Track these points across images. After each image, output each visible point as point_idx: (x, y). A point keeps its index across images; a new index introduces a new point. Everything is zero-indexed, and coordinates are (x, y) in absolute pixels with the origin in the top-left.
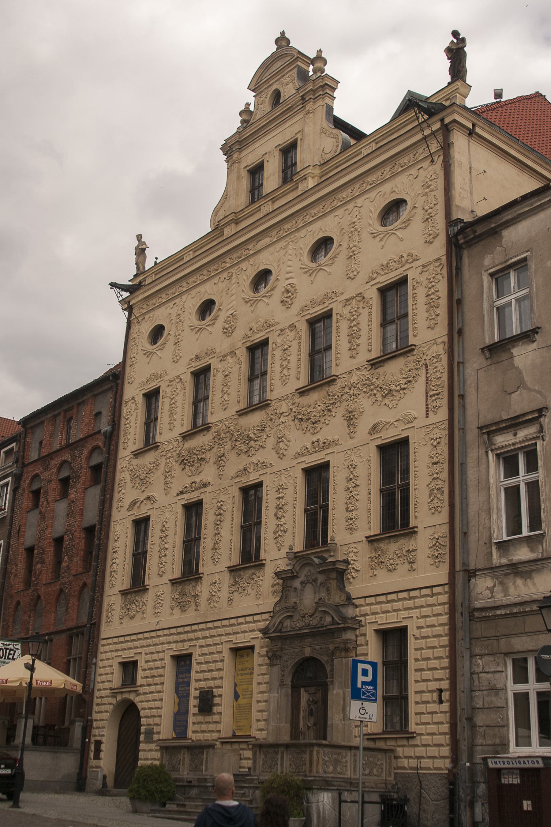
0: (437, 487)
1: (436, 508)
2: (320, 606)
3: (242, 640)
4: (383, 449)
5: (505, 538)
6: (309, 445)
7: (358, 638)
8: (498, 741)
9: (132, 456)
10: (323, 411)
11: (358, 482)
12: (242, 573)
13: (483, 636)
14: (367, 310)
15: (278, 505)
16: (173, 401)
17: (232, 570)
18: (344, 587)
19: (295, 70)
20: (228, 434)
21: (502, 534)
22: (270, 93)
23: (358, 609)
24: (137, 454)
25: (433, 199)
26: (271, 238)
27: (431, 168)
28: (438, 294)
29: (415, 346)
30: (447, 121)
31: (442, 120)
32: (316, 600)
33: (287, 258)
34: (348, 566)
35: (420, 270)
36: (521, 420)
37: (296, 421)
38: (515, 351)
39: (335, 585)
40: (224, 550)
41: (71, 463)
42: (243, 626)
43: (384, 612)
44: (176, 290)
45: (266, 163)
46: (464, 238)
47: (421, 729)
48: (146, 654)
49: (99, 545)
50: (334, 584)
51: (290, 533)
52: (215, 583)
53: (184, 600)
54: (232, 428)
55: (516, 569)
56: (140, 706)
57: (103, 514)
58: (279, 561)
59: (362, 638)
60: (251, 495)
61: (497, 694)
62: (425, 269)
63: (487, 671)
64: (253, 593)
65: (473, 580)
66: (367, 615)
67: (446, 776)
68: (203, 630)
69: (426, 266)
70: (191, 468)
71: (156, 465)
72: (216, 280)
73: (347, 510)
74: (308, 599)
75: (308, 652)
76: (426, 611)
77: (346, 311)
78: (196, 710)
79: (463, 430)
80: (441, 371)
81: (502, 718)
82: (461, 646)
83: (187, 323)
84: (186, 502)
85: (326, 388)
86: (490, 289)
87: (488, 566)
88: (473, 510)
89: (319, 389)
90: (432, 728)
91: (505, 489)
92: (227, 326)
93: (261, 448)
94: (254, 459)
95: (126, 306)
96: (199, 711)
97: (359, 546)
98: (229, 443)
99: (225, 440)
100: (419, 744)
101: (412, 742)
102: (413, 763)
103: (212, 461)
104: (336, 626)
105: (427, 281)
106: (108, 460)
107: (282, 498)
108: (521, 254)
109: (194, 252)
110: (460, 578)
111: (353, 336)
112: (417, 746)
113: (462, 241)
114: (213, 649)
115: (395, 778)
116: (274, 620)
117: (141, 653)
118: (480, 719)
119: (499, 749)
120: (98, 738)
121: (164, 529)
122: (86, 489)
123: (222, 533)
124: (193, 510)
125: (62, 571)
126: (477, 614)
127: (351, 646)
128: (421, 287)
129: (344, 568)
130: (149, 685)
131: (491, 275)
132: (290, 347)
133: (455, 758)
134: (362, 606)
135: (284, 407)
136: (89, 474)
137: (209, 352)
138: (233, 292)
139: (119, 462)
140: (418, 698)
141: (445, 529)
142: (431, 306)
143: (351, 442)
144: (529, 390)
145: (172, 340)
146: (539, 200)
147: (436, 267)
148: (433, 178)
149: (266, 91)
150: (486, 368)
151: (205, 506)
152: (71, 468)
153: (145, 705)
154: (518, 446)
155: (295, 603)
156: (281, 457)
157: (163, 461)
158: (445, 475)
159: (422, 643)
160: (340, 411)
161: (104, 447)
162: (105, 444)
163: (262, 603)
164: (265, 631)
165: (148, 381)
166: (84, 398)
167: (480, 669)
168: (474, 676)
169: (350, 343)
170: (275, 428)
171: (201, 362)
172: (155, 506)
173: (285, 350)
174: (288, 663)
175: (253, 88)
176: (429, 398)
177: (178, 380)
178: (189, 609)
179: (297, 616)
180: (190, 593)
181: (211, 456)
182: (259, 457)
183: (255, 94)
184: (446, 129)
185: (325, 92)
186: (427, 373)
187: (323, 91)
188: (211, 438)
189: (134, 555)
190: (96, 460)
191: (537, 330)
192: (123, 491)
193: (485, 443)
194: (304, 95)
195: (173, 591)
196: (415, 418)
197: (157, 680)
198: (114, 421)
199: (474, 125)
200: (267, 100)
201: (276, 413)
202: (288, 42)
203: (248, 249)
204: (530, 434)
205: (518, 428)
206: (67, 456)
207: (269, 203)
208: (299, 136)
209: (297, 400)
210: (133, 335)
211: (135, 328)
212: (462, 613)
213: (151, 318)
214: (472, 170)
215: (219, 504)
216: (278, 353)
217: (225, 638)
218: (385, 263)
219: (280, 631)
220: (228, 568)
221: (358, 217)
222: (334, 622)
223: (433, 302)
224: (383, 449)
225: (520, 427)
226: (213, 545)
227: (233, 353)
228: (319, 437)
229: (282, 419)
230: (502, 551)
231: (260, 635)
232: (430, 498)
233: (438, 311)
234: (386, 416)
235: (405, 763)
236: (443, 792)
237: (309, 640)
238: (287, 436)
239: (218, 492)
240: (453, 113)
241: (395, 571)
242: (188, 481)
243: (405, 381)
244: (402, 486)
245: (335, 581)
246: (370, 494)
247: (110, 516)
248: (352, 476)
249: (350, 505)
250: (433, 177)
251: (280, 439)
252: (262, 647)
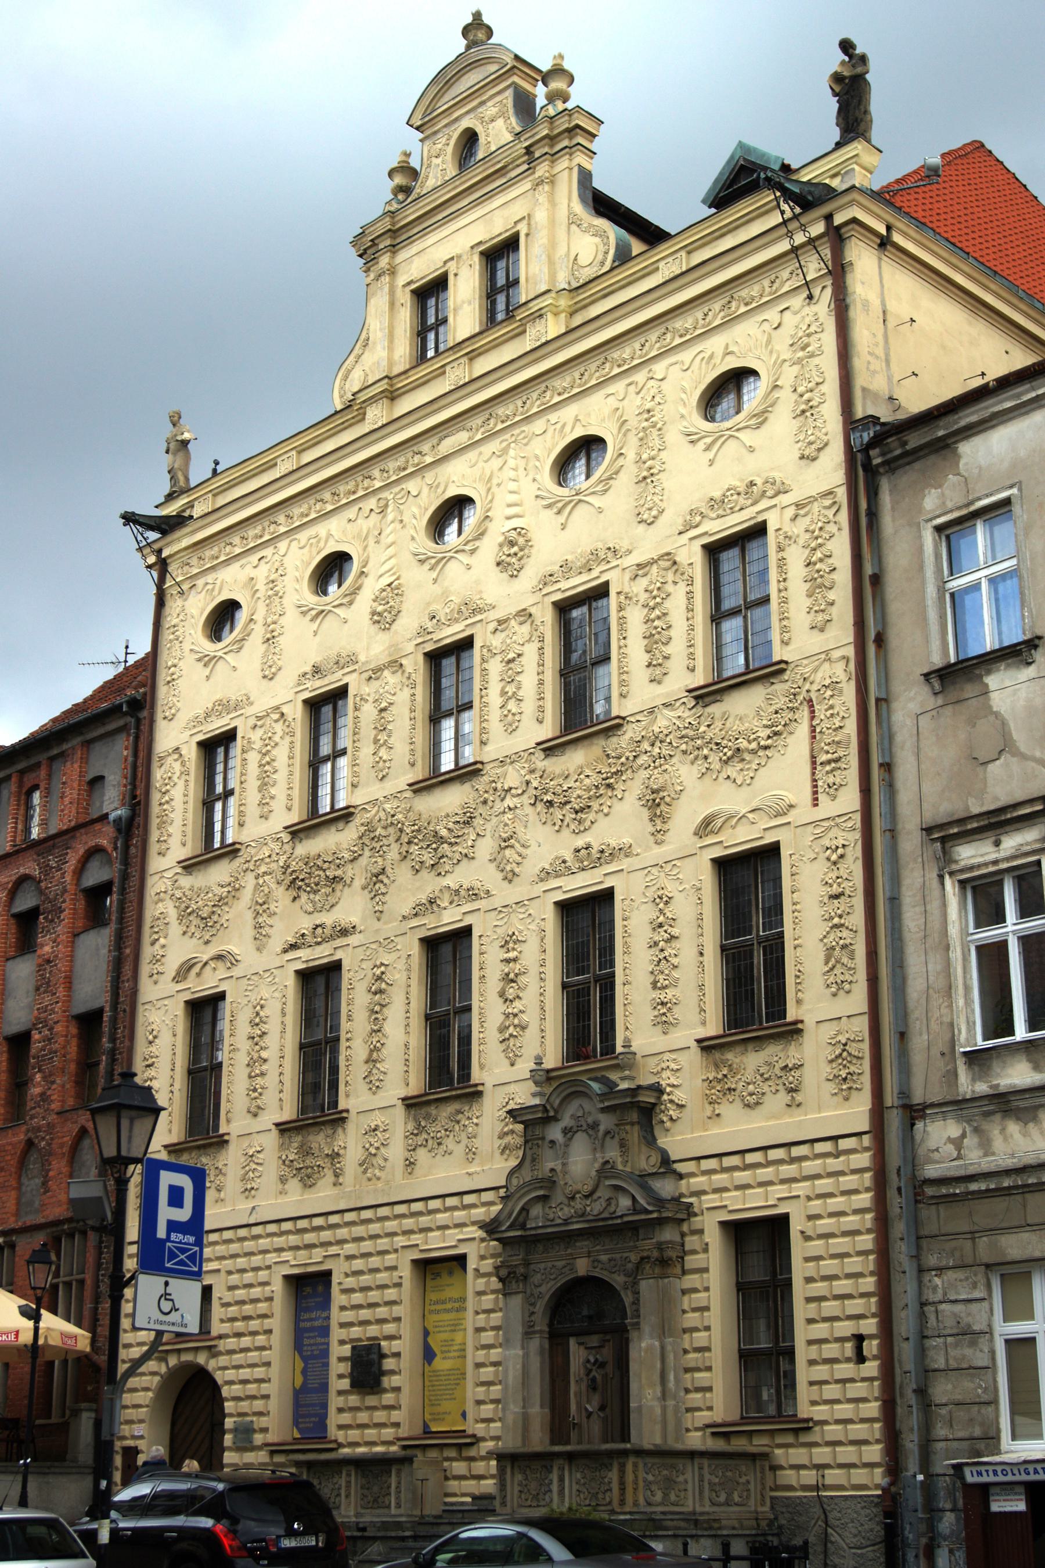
0: (842, 942)
1: (840, 984)
2: (606, 1178)
3: (438, 1244)
4: (724, 865)
5: (981, 1043)
6: (568, 856)
7: (687, 1239)
8: (977, 1432)
9: (179, 870)
10: (597, 787)
11: (675, 931)
12: (433, 1110)
13: (943, 1232)
14: (682, 589)
15: (507, 975)
16: (267, 759)
17: (411, 1104)
18: (655, 1139)
19: (509, 93)
20: (391, 830)
21: (974, 1035)
22: (456, 135)
23: (684, 1182)
24: (189, 866)
25: (814, 373)
26: (471, 434)
27: (807, 310)
28: (830, 561)
29: (786, 662)
30: (838, 220)
31: (829, 218)
32: (597, 1166)
33: (507, 474)
34: (659, 1098)
35: (791, 512)
36: (1009, 816)
37: (540, 806)
38: (993, 681)
39: (636, 1135)
40: (392, 1062)
41: (40, 881)
42: (439, 1216)
43: (738, 1188)
44: (264, 529)
45: (451, 278)
46: (883, 454)
47: (820, 1412)
48: (230, 1273)
49: (112, 1053)
50: (634, 1134)
51: (533, 1031)
52: (375, 1130)
53: (308, 1163)
54: (400, 816)
55: (1006, 1104)
56: (219, 1377)
57: (118, 988)
58: (513, 1086)
59: (695, 1238)
60: (447, 954)
61: (973, 1344)
62: (802, 512)
63: (952, 1298)
64: (459, 1150)
65: (919, 1125)
66: (704, 1192)
67: (876, 1500)
68: (353, 1223)
69: (804, 506)
70: (312, 896)
71: (234, 890)
72: (351, 513)
73: (654, 985)
74: (580, 1162)
75: (582, 1267)
76: (824, 1185)
77: (639, 587)
78: (345, 1384)
79: (892, 832)
80: (842, 714)
81: (986, 1388)
82: (901, 1253)
83: (290, 600)
84: (304, 966)
85: (601, 742)
86: (938, 556)
87: (949, 1098)
88: (915, 987)
89: (586, 743)
90: (844, 1410)
91: (979, 948)
92: (380, 609)
93: (465, 861)
94: (450, 881)
95: (152, 559)
96: (352, 1385)
97: (683, 1058)
98: (395, 847)
99: (385, 842)
100: (819, 1440)
101: (804, 1438)
102: (809, 1477)
103: (358, 883)
104: (643, 1217)
105: (808, 536)
106: (125, 876)
107: (515, 960)
108: (998, 491)
109: (299, 453)
110: (894, 1121)
111: (656, 640)
112: (816, 1444)
113: (877, 461)
114: (375, 1262)
115: (772, 1508)
116: (510, 1204)
117: (218, 1271)
118: (942, 1391)
119: (981, 1445)
120: (130, 1443)
121: (257, 1020)
122: (76, 935)
123: (387, 1028)
124: (320, 983)
125: (30, 1104)
126: (930, 1191)
127: (672, 1254)
128: (794, 546)
129: (652, 1101)
130: (238, 1335)
131: (939, 529)
132: (519, 655)
133: (894, 1465)
134: (692, 1175)
135: (513, 777)
136: (81, 905)
137: (342, 661)
138: (390, 540)
139: (150, 881)
140: (813, 1352)
141: (861, 1026)
142: (817, 584)
143: (657, 850)
144: (1024, 757)
145: (259, 632)
146: (1033, 389)
147: (825, 508)
148: (812, 329)
149: (446, 131)
150: (934, 713)
151: (346, 976)
152: (41, 892)
153: (230, 1374)
154: (1004, 866)
155: (552, 1170)
156: (510, 877)
157: (249, 882)
158: (857, 919)
159: (817, 1247)
160: (633, 788)
161: (115, 848)
162: (115, 844)
163: (478, 1169)
164: (491, 1228)
165: (207, 715)
166: (65, 747)
167: (939, 1296)
168: (925, 1308)
169: (648, 652)
170: (494, 820)
171: (326, 681)
172: (236, 972)
173: (509, 662)
174: (543, 1289)
175: (419, 123)
176: (819, 768)
177: (276, 716)
178: (320, 1183)
179: (558, 1197)
180: (320, 1149)
181: (358, 874)
182: (460, 877)
183: (421, 136)
184: (837, 236)
185: (575, 142)
186: (812, 718)
187: (571, 139)
188: (355, 836)
189: (190, 1072)
190: (95, 875)
191: (1037, 642)
192: (162, 941)
193: (938, 859)
194: (531, 146)
195: (282, 1147)
196: (791, 806)
197: (254, 1325)
198: (134, 797)
199: (889, 228)
200: (450, 149)
201: (495, 789)
202: (489, 32)
203: (420, 453)
204: (1027, 844)
205: (1002, 830)
206: (30, 867)
207: (462, 360)
208: (523, 228)
209: (540, 762)
210: (171, 617)
211: (174, 606)
212: (899, 1189)
213: (209, 587)
214: (889, 318)
215: (378, 972)
216: (495, 667)
217: (400, 1241)
218: (717, 494)
219: (523, 1227)
220: (403, 1099)
221: (657, 399)
222: (636, 1208)
223: (822, 577)
224: (724, 865)
225: (1007, 828)
226: (367, 1052)
227: (396, 665)
228: (588, 840)
229: (509, 801)
230: (976, 1068)
231: (480, 1234)
232: (826, 963)
233: (831, 595)
234: (728, 799)
235: (788, 1477)
236: (872, 1530)
237: (584, 1245)
238: (520, 835)
239: (374, 946)
240: (851, 203)
241: (760, 1107)
242: (305, 924)
243: (768, 732)
244: (767, 939)
245: (636, 1128)
246: (701, 954)
247: (134, 992)
248: (661, 919)
249: (661, 977)
250: (812, 329)
251: (506, 842)
252: (483, 1258)
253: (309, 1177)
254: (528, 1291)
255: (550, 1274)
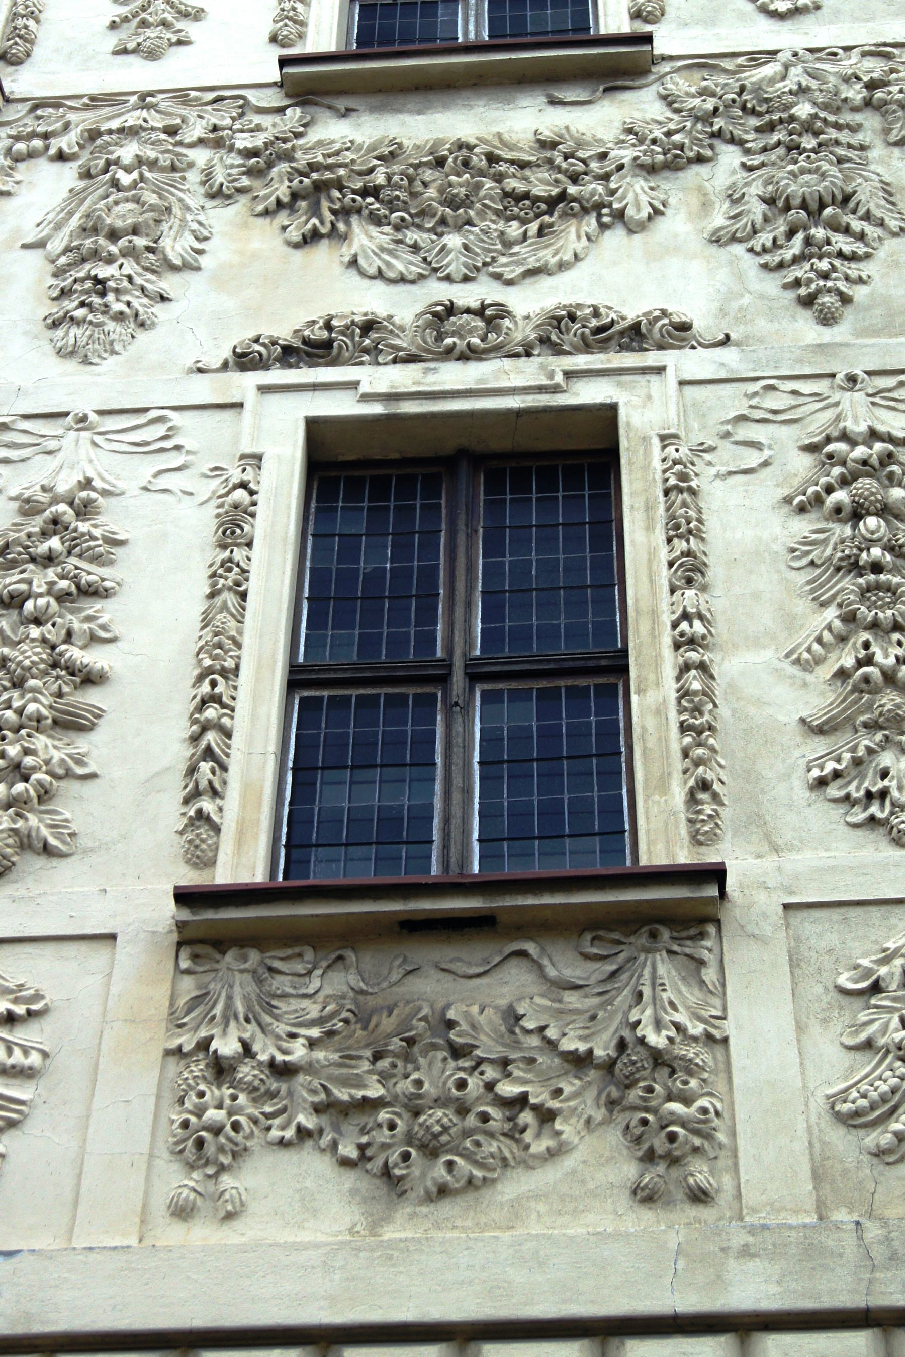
70: (412, 236)
84: (377, 409)
178: (513, 1187)
239: (820, 387)
253: (431, 1151)
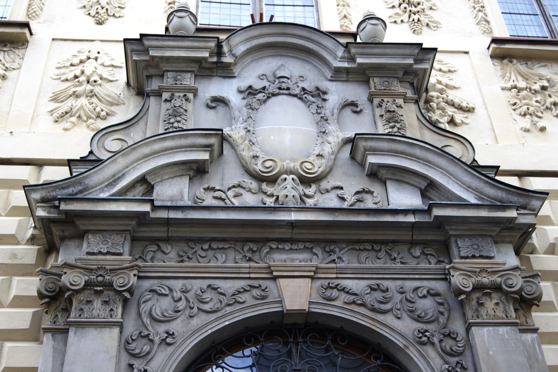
75: (296, 296)
174: (176, 326)
254: (131, 327)
255: (198, 300)
